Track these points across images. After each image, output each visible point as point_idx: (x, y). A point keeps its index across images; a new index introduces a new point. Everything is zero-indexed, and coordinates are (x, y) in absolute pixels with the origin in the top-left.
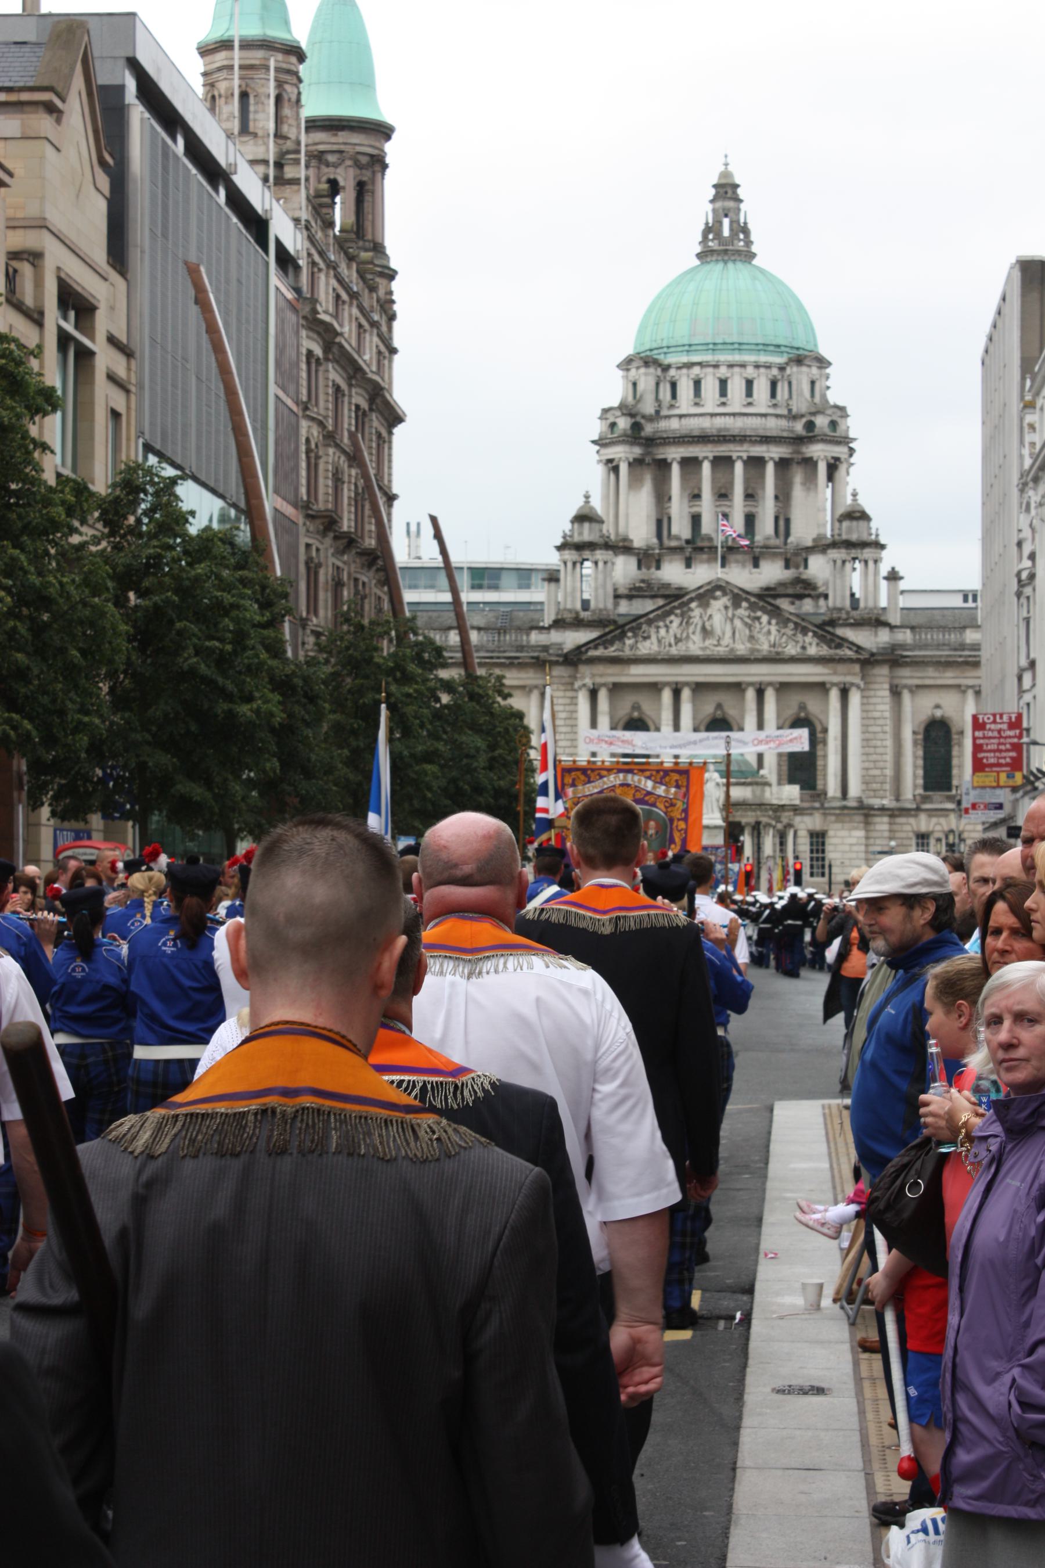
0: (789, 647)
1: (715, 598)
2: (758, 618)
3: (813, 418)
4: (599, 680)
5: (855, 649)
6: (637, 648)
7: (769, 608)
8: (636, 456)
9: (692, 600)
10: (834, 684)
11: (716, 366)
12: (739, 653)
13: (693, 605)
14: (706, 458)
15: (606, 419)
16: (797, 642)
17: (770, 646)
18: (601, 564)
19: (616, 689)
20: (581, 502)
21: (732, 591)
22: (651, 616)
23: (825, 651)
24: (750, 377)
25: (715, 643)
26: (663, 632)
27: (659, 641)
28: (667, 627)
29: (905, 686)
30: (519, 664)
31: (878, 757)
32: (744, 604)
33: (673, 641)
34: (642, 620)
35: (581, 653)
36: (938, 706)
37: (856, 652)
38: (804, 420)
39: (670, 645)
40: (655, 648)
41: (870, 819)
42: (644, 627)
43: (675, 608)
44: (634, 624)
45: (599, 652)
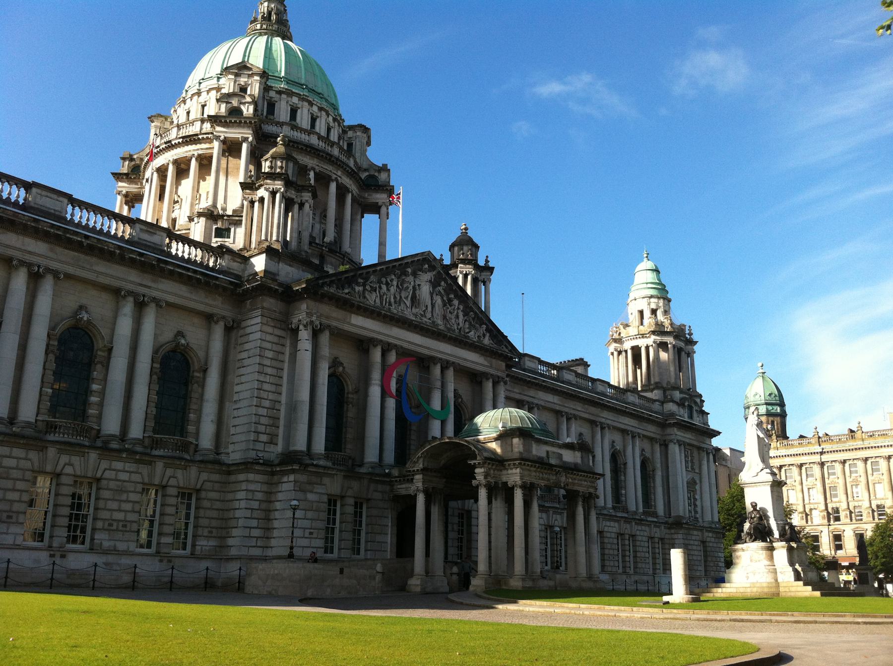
0: (472, 333)
1: (421, 270)
2: (450, 301)
3: (376, 174)
4: (324, 321)
5: (510, 348)
6: (365, 297)
7: (460, 293)
11: (311, 104)
12: (440, 327)
13: (409, 270)
14: (313, 169)
15: (227, 103)
16: (476, 329)
17: (458, 329)
19: (338, 335)
25: (423, 313)
26: (384, 287)
27: (381, 297)
28: (387, 284)
30: (217, 286)
32: (443, 283)
33: (392, 300)
34: (371, 270)
38: (367, 174)
39: (390, 304)
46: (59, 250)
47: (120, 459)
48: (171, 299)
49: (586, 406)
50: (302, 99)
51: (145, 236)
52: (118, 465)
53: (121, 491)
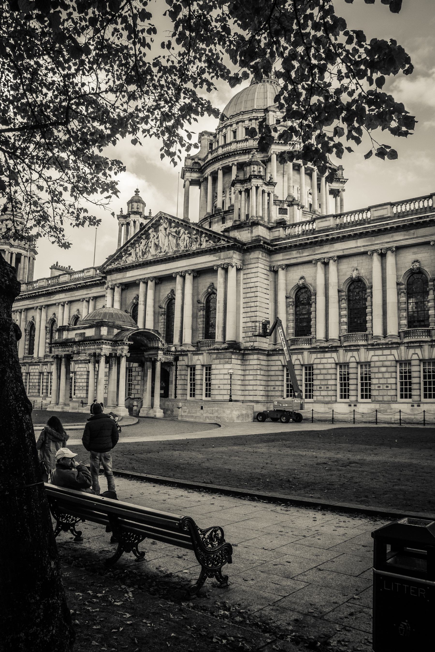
4: (114, 283)
5: (226, 239)
8: (193, 178)
9: (149, 228)
10: (218, 266)
13: (150, 231)
14: (218, 169)
18: (132, 223)
20: (134, 194)
21: (167, 218)
22: (132, 241)
23: (211, 244)
24: (246, 126)
26: (138, 249)
29: (280, 266)
31: (253, 314)
35: (105, 268)
36: (302, 278)
37: (228, 242)
40: (134, 260)
41: (247, 357)
42: (129, 248)
43: (142, 234)
44: (125, 248)
45: (114, 266)
46: (67, 293)
47: (81, 363)
48: (95, 295)
49: (412, 231)
50: (226, 127)
51: (88, 274)
52: (80, 365)
53: (82, 375)
